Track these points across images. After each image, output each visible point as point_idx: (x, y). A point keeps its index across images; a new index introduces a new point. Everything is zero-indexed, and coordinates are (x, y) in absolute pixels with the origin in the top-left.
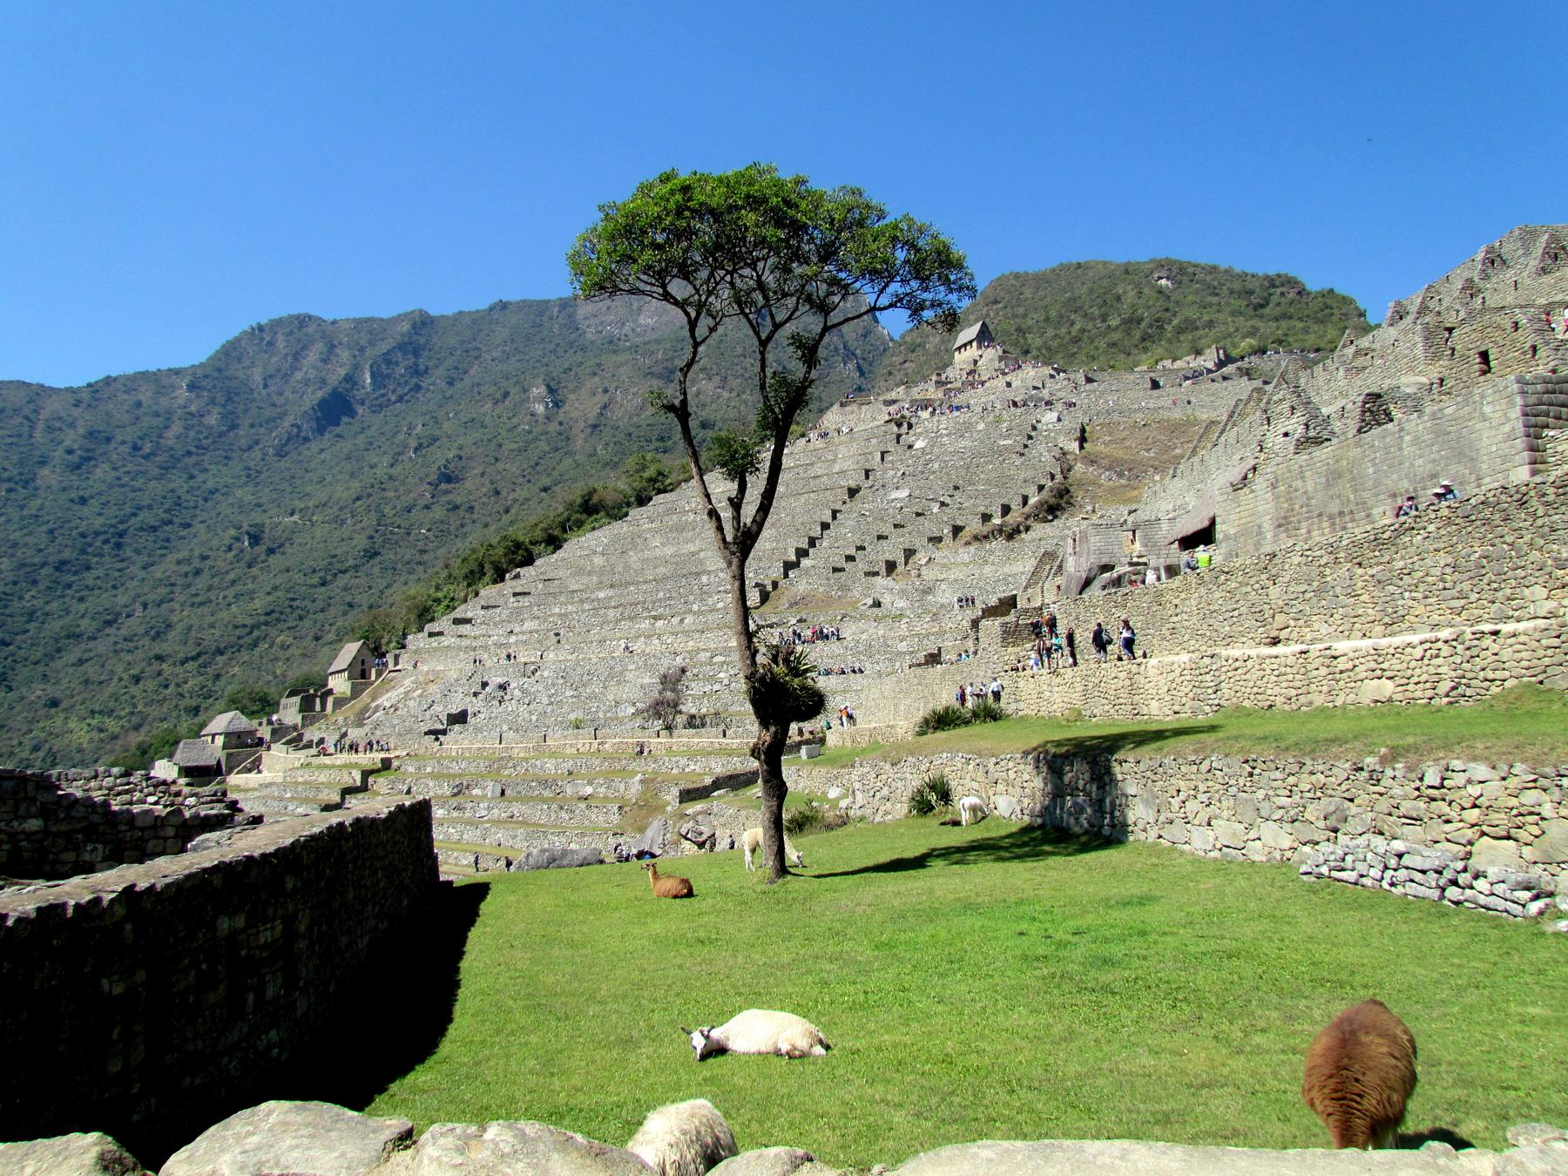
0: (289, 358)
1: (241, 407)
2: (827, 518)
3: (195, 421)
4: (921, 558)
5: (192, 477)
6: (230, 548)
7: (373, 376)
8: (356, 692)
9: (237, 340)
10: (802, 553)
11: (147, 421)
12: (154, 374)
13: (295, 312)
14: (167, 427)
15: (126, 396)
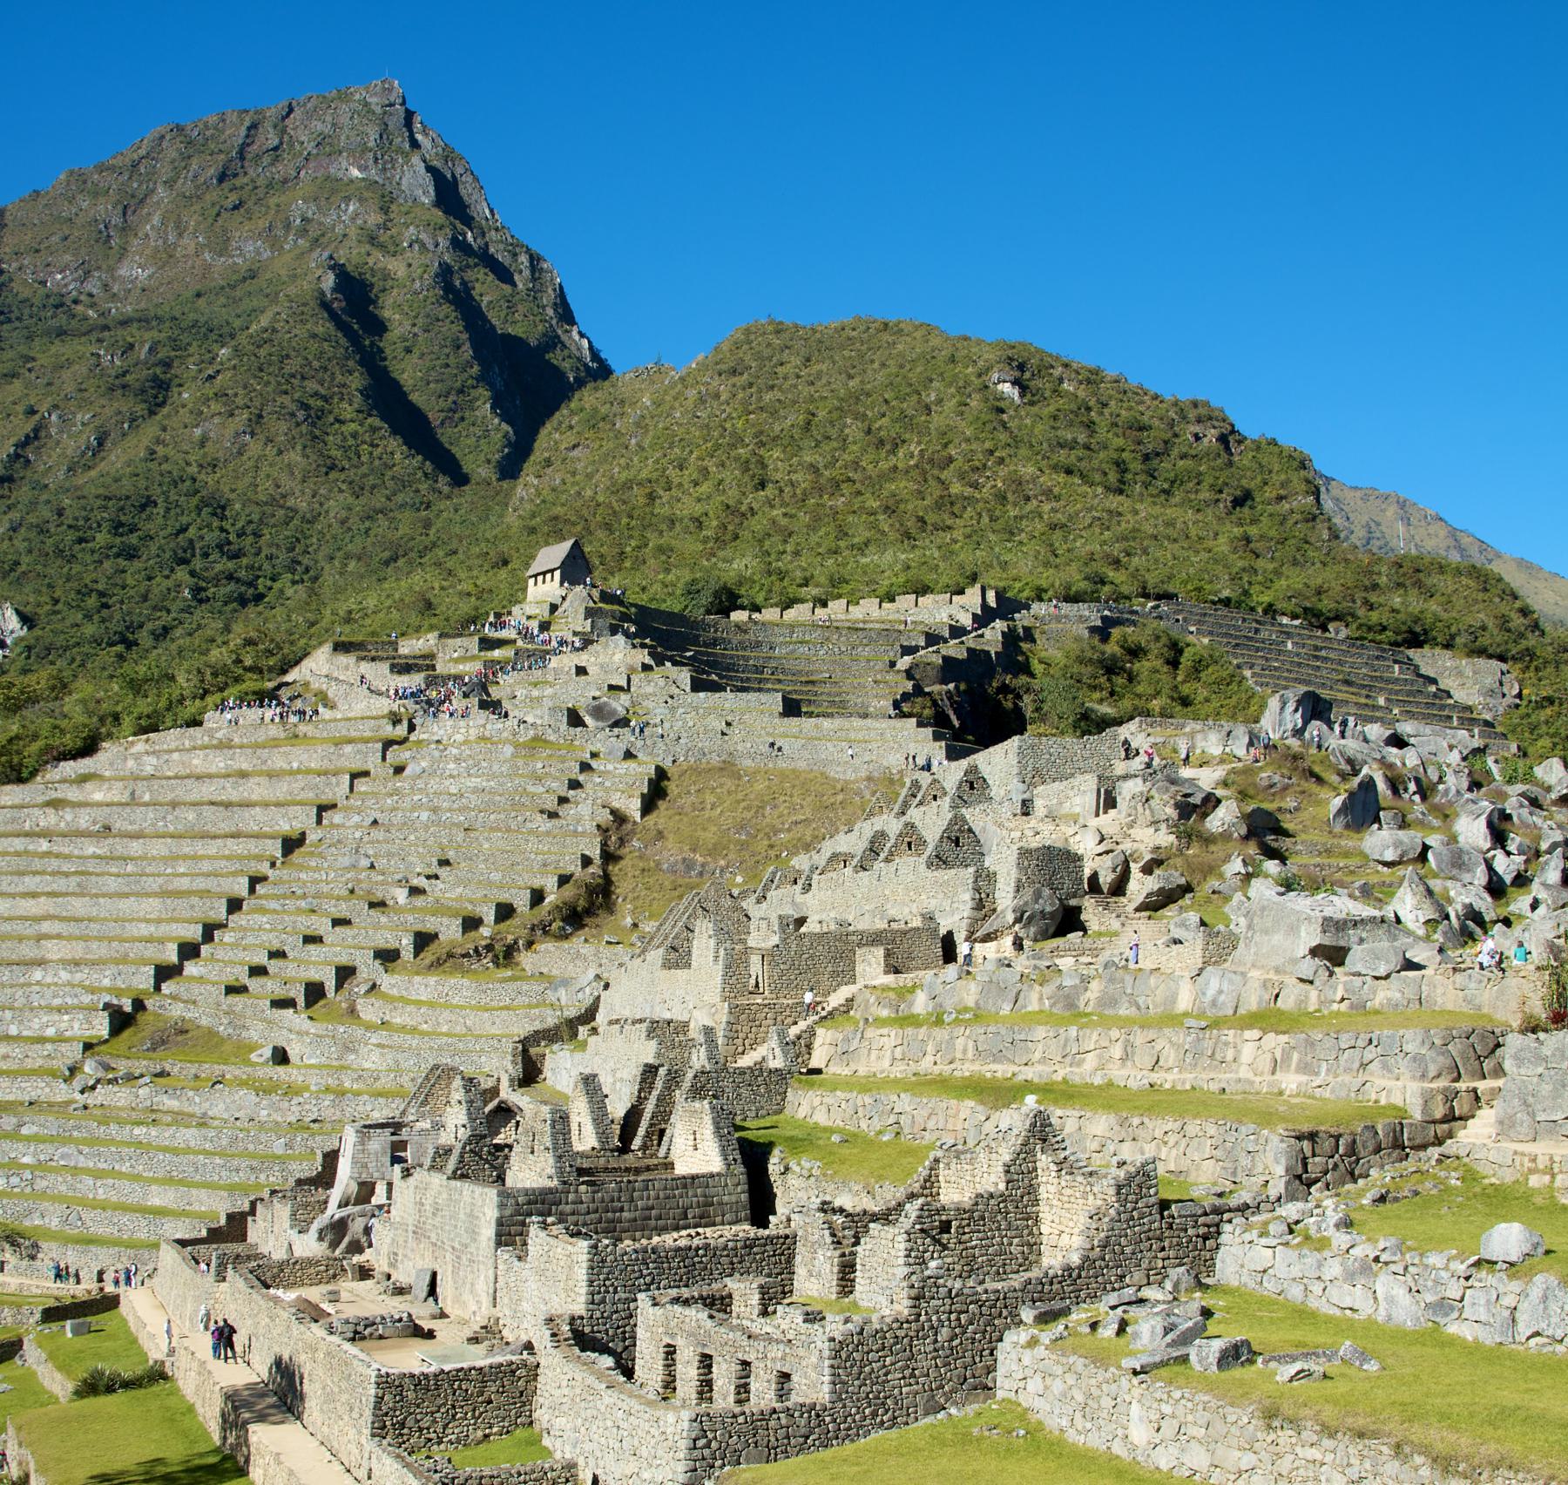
2: (240, 887)
4: (358, 986)
10: (189, 951)
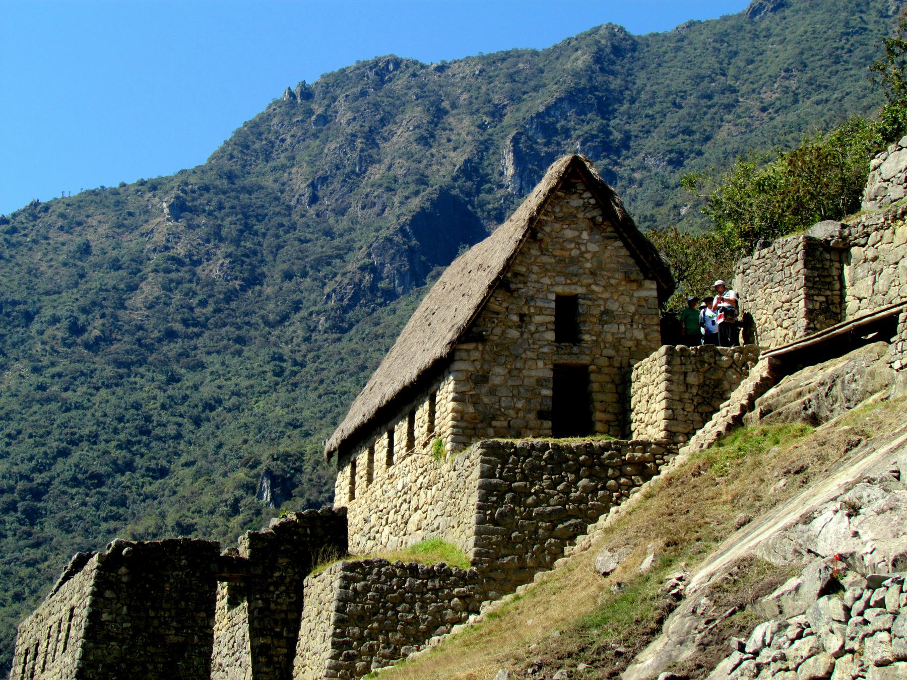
0: (359, 143)
1: (268, 242)
3: (184, 273)
5: (173, 379)
6: (235, 509)
7: (517, 153)
8: (522, 530)
9: (265, 118)
11: (97, 279)
12: (115, 192)
13: (370, 58)
14: (133, 288)
15: (64, 237)
